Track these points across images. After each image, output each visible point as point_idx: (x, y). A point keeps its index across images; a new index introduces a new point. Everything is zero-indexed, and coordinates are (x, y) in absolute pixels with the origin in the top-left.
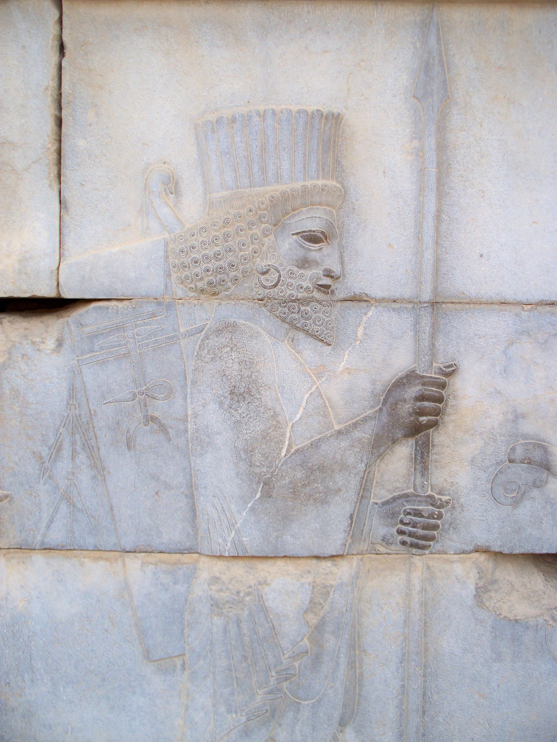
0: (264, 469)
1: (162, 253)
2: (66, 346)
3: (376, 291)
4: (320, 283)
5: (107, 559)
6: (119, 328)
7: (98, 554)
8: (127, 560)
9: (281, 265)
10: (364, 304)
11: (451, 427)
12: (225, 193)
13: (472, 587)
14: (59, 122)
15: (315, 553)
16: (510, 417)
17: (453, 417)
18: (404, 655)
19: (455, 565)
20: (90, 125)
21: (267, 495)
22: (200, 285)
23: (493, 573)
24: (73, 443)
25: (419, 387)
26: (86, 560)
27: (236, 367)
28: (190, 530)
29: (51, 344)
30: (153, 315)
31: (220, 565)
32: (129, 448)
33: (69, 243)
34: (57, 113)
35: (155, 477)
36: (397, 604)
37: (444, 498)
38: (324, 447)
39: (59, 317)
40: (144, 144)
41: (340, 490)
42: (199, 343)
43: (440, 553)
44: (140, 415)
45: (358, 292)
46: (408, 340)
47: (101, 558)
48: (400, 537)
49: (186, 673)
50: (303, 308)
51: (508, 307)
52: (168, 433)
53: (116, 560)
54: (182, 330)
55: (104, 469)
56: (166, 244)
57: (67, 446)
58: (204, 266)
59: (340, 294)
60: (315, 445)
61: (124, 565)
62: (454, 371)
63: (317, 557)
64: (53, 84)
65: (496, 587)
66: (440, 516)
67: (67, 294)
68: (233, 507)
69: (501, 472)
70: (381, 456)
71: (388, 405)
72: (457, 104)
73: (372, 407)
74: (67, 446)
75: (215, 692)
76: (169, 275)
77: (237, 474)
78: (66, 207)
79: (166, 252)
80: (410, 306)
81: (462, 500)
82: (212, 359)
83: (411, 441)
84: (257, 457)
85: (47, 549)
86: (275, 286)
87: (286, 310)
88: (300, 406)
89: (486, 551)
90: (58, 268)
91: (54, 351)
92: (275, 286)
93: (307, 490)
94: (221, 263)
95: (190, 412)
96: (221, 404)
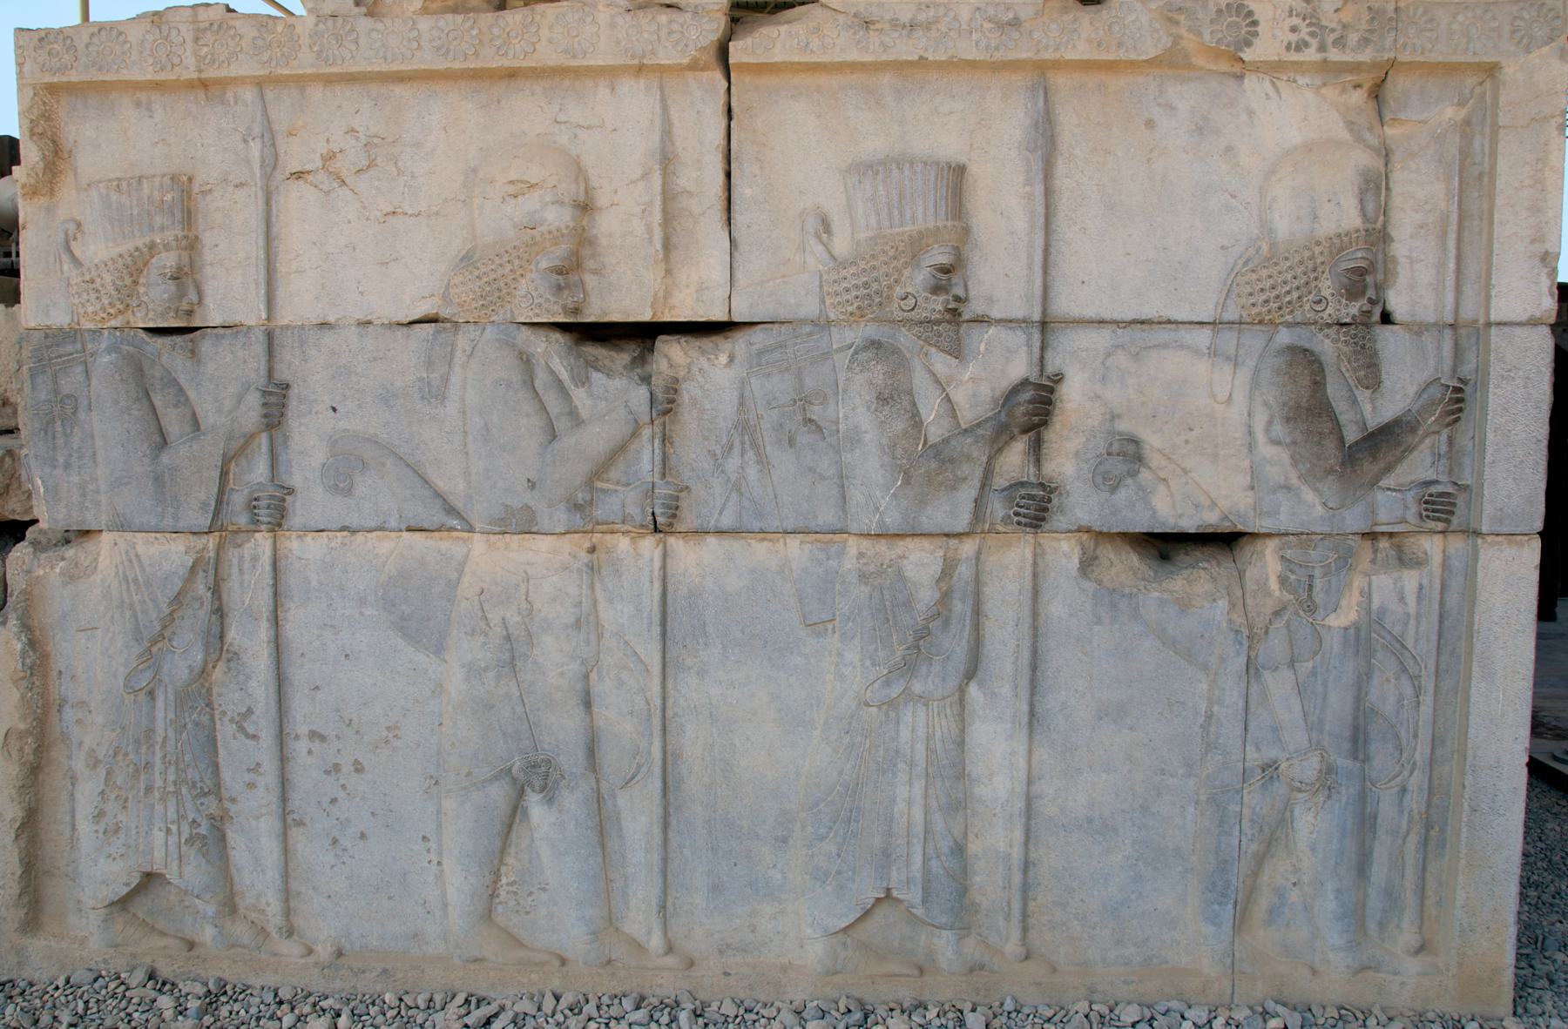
0: (904, 461)
1: (817, 283)
2: (736, 361)
3: (996, 313)
4: (950, 307)
5: (770, 540)
6: (782, 346)
7: (762, 535)
8: (788, 540)
9: (918, 292)
10: (986, 324)
11: (1058, 426)
12: (871, 234)
13: (1077, 561)
14: (728, 175)
15: (946, 530)
16: (1108, 417)
17: (1060, 418)
18: (1019, 619)
19: (1062, 543)
20: (755, 176)
21: (907, 482)
22: (850, 309)
23: (1095, 550)
24: (743, 443)
25: (1032, 392)
26: (753, 541)
27: (881, 376)
28: (841, 513)
29: (723, 359)
30: (810, 335)
31: (866, 544)
32: (791, 446)
33: (739, 275)
34: (727, 167)
35: (812, 470)
36: (1014, 575)
37: (1053, 485)
38: (953, 442)
39: (726, 338)
40: (801, 192)
41: (966, 478)
42: (849, 357)
43: (1049, 532)
44: (800, 418)
45: (980, 313)
46: (1023, 355)
47: (764, 539)
48: (1016, 519)
49: (837, 635)
50: (935, 328)
51: (1106, 325)
52: (823, 433)
53: (778, 540)
54: (835, 347)
55: (768, 464)
56: (821, 276)
57: (737, 445)
58: (854, 294)
59: (966, 316)
60: (946, 441)
61: (785, 544)
62: (1060, 379)
63: (947, 535)
64: (723, 142)
65: (1097, 562)
66: (1050, 501)
67: (736, 319)
68: (878, 493)
69: (1100, 463)
70: (1000, 450)
71: (1006, 408)
72: (1062, 154)
73: (993, 409)
74: (737, 445)
75: (862, 648)
76: (824, 302)
77: (882, 466)
78: (735, 246)
79: (821, 282)
80: (1023, 325)
81: (1068, 487)
82: (861, 371)
83: (1025, 438)
84: (899, 451)
85: (720, 532)
86: (913, 309)
87: (922, 329)
88: (933, 409)
89: (1088, 531)
90: (730, 297)
91: (726, 366)
92: (913, 309)
93: (940, 478)
94: (868, 291)
95: (841, 415)
96: (869, 408)
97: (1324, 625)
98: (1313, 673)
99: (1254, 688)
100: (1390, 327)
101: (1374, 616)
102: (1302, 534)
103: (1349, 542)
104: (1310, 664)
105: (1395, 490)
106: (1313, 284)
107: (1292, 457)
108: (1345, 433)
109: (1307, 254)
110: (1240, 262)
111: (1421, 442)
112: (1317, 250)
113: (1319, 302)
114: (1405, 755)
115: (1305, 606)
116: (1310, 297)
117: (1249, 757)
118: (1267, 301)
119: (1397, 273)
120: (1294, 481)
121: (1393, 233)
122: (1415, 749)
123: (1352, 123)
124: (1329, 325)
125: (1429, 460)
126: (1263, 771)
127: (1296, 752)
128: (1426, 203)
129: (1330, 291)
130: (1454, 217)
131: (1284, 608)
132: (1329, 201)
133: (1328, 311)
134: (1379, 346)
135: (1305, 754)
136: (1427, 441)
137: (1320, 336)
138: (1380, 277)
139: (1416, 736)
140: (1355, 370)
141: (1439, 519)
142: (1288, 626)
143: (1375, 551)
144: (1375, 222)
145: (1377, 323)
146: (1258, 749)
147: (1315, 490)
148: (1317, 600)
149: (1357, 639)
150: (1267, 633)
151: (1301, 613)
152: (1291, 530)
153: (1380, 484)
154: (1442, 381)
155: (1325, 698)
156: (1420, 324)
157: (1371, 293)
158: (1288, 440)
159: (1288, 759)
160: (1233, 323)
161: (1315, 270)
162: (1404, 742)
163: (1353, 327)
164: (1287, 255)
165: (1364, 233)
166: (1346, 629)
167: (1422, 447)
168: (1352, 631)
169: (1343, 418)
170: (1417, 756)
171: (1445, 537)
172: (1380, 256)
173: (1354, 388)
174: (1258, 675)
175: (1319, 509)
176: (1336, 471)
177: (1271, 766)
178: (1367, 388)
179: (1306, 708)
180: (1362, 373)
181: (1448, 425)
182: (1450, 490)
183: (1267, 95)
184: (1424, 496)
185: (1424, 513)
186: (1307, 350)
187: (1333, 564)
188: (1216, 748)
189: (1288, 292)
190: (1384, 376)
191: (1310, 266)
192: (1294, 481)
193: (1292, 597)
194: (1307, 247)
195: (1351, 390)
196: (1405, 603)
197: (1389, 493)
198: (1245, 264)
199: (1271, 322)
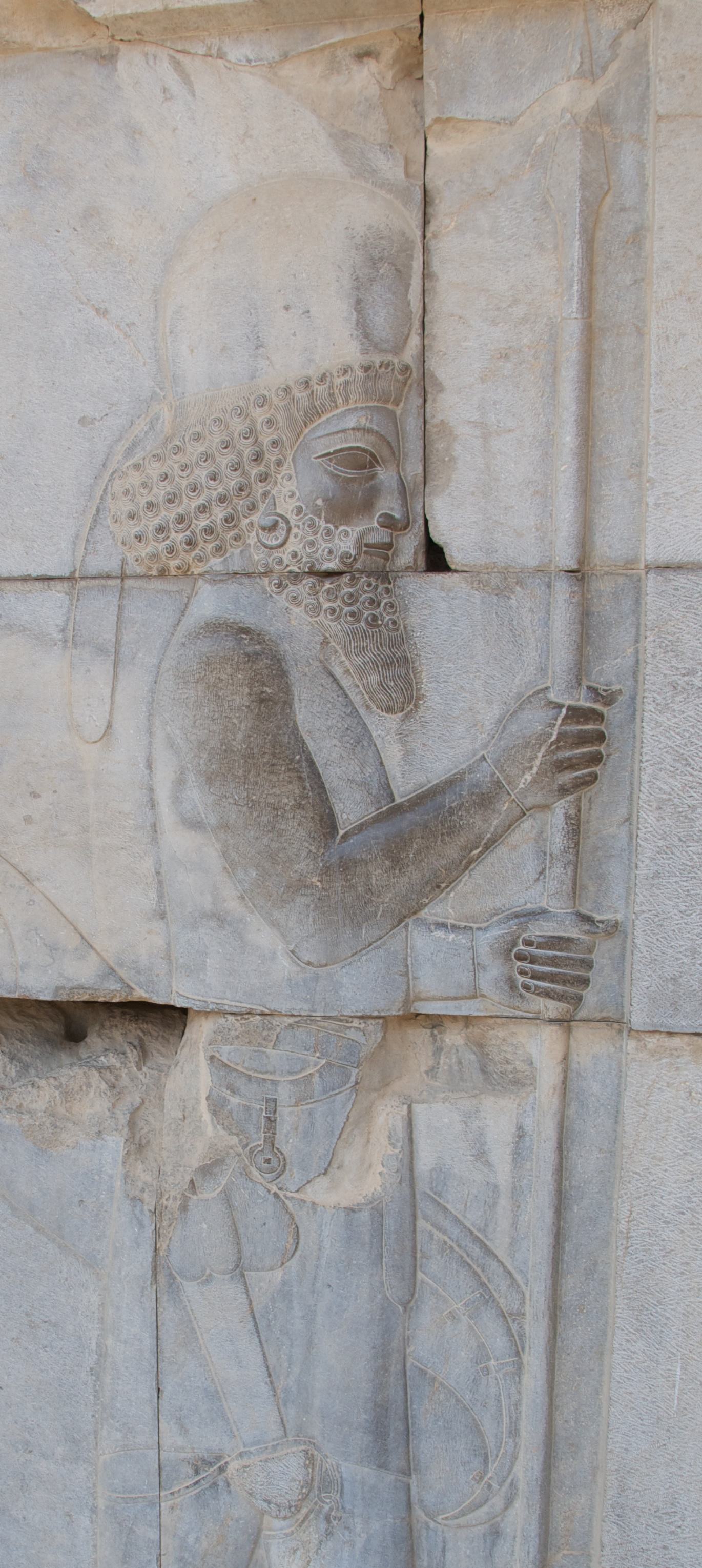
97: (304, 1201)
98: (284, 1293)
99: (169, 1314)
100: (438, 578)
101: (422, 1186)
102: (250, 1013)
103: (352, 1034)
104: (278, 1275)
105: (454, 928)
106: (259, 489)
107: (225, 854)
108: (338, 808)
109: (238, 426)
110: (121, 448)
111: (509, 827)
112: (260, 415)
113: (274, 527)
114: (492, 1468)
115: (260, 1159)
116: (255, 518)
117: (166, 1442)
118: (161, 529)
119: (453, 459)
120: (233, 905)
121: (441, 369)
122: (514, 1458)
123: (347, 135)
124: (296, 577)
125: (531, 868)
126: (197, 1472)
127: (254, 1444)
128: (515, 302)
129: (293, 503)
130: (572, 331)
131: (219, 1162)
132: (287, 308)
133: (290, 547)
134: (413, 619)
135: (274, 1448)
136: (526, 824)
137: (282, 600)
138: (413, 469)
139: (514, 1432)
140: (361, 671)
141: (547, 994)
142: (227, 1197)
143: (438, 1051)
144: (398, 349)
145: (407, 569)
146: (183, 1429)
147: (274, 924)
148: (286, 1150)
149: (378, 1231)
150: (184, 1208)
151: (255, 1173)
152: (229, 1003)
153: (424, 913)
154: (552, 696)
155: (310, 1344)
156: (505, 572)
157: (389, 504)
158: (213, 820)
159: (241, 1455)
160: (108, 577)
161: (258, 458)
162: (491, 1443)
163: (346, 579)
164: (198, 429)
165: (360, 373)
166: (350, 1211)
167: (515, 837)
168: (365, 1216)
169: (332, 776)
170: (519, 1470)
171: (569, 1031)
172: (412, 426)
173: (362, 711)
174: (174, 1288)
175: (284, 966)
176: (312, 886)
177: (210, 1464)
178: (389, 710)
179: (272, 1361)
180: (374, 678)
181: (563, 791)
182: (573, 932)
183: (165, 90)
184: (515, 944)
185: (521, 979)
186: (246, 631)
187: (316, 1079)
188: (113, 1417)
189: (203, 509)
190: (427, 685)
191: (247, 453)
192: (233, 905)
193: (234, 1140)
194: (241, 413)
195: (355, 713)
196: (488, 1164)
197: (440, 934)
198: (130, 451)
199: (185, 572)
